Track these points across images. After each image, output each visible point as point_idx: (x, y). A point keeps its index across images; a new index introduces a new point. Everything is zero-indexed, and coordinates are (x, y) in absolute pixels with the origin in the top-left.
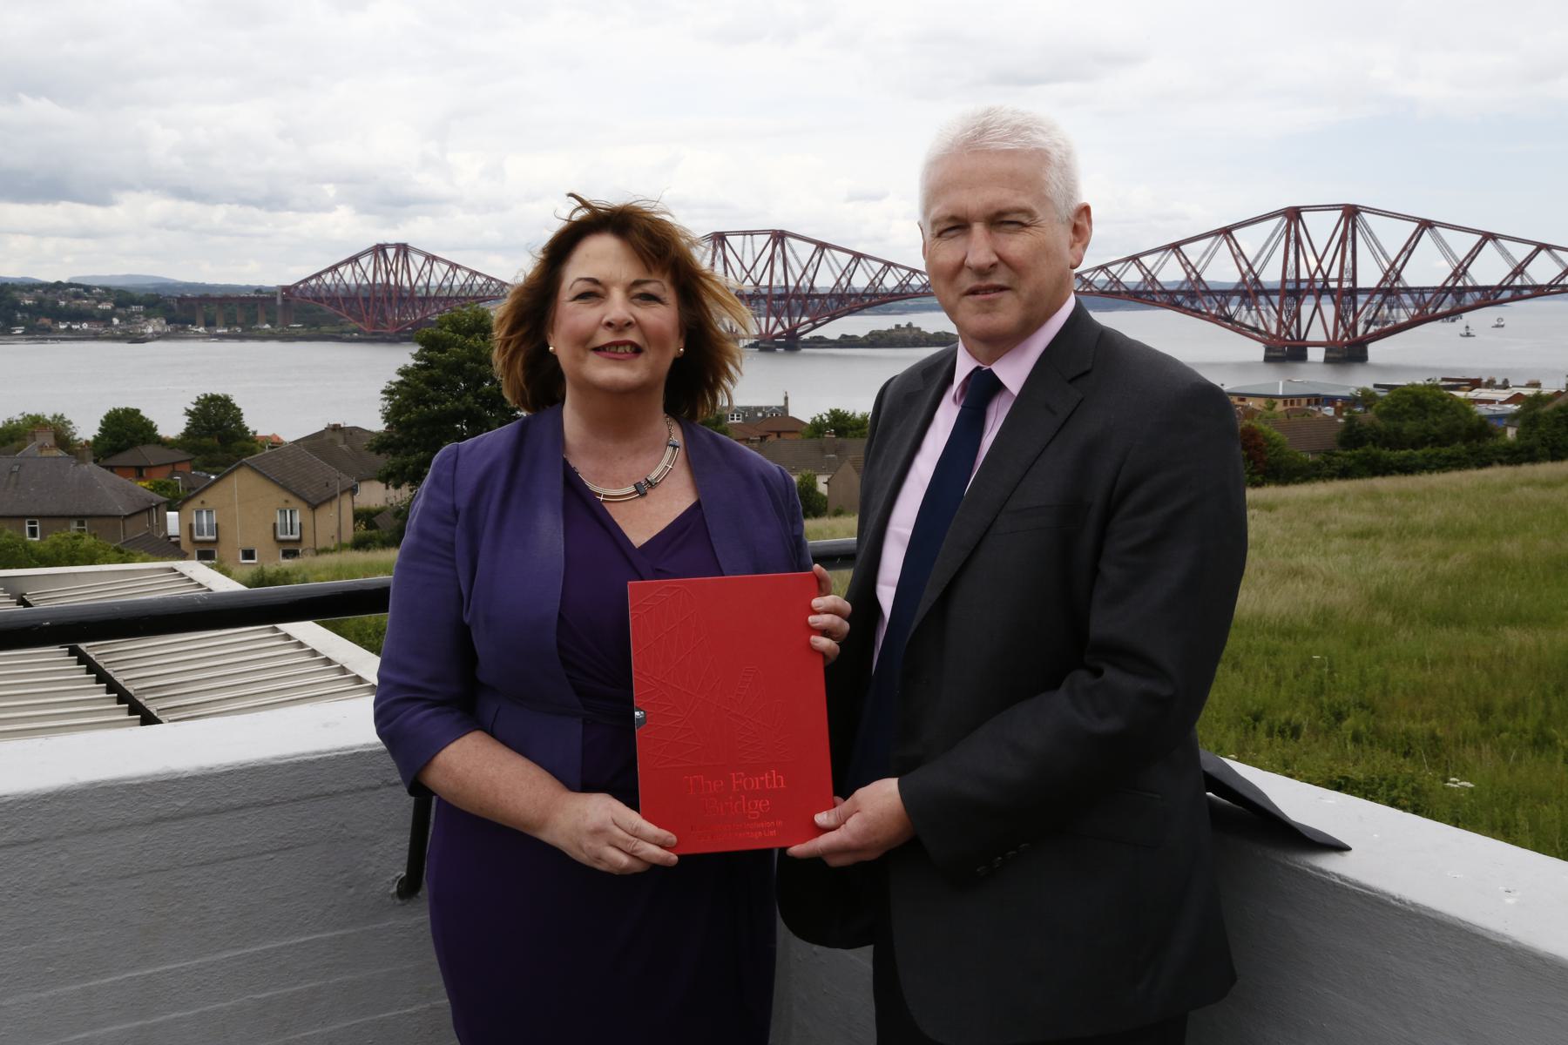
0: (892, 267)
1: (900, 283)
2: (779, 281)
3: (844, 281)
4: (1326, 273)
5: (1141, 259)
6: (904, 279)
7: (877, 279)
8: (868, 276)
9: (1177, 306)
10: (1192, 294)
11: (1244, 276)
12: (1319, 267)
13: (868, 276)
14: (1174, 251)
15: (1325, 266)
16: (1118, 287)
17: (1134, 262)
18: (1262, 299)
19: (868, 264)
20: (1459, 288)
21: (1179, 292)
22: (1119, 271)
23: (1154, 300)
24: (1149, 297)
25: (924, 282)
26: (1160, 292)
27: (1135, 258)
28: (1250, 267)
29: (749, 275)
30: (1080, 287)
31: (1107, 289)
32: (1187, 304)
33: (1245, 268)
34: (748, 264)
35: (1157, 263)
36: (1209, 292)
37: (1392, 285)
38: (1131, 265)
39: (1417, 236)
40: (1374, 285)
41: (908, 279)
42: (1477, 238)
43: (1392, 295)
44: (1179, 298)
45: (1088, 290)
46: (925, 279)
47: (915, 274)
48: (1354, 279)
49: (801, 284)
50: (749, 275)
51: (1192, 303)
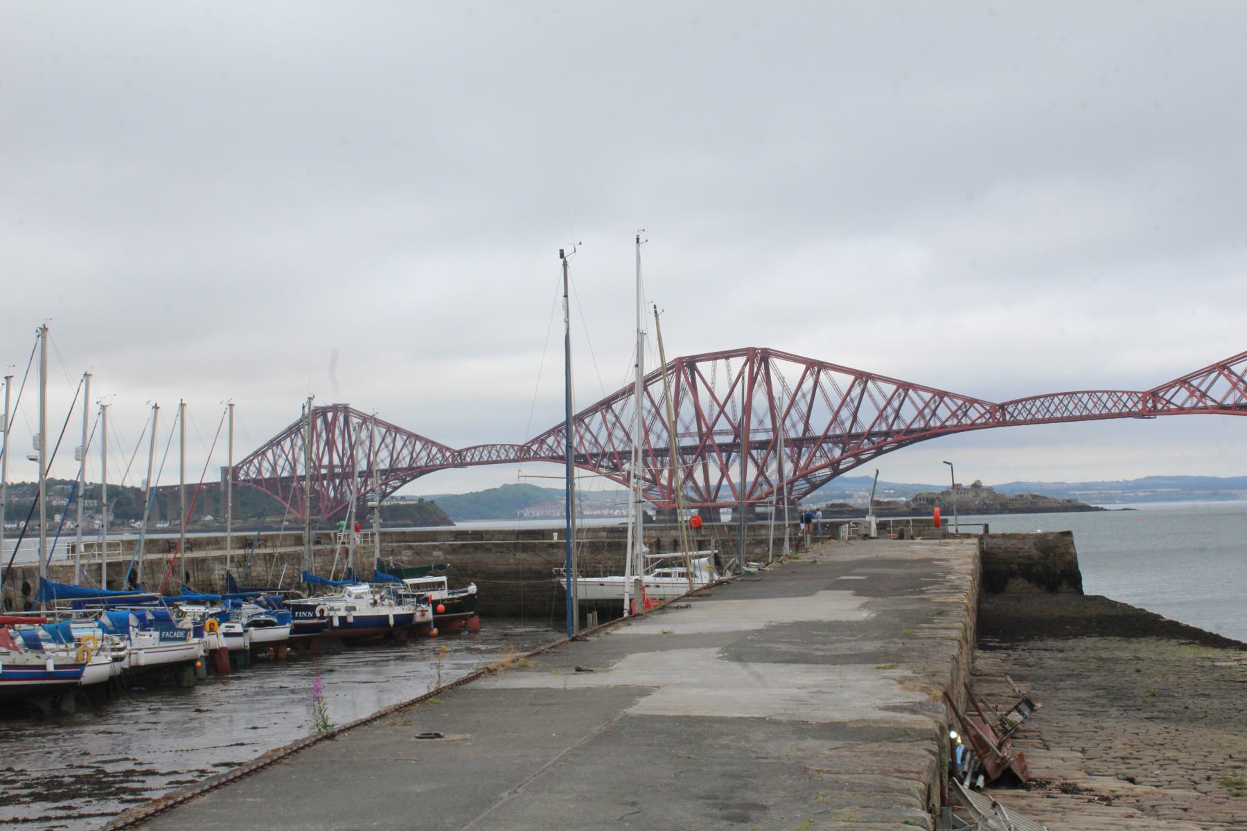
0: (911, 392)
1: (921, 413)
2: (761, 422)
3: (845, 414)
6: (927, 405)
7: (889, 410)
8: (915, 406)
13: (915, 406)
19: (878, 388)
25: (954, 408)
29: (722, 411)
30: (1187, 400)
34: (721, 395)
41: (933, 407)
45: (1201, 405)
46: (955, 404)
49: (788, 423)
50: (722, 411)
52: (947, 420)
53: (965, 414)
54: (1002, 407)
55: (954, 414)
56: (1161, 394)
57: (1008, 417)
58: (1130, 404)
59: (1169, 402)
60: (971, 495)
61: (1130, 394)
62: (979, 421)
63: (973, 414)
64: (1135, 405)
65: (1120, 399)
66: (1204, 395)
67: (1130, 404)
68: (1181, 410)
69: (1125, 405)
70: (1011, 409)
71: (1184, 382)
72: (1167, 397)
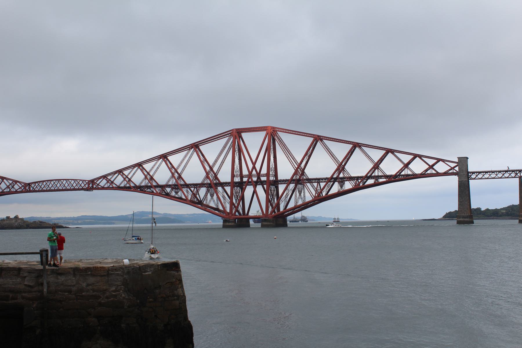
4: (258, 171)
5: (144, 166)
9: (168, 195)
10: (176, 187)
11: (207, 174)
12: (254, 167)
14: (164, 160)
15: (258, 166)
16: (129, 184)
17: (139, 168)
18: (220, 189)
20: (341, 178)
21: (169, 186)
22: (129, 174)
23: (153, 192)
24: (149, 190)
25: (8, 184)
26: (156, 187)
27: (139, 165)
28: (211, 168)
31: (122, 185)
32: (173, 194)
33: (208, 168)
35: (153, 167)
36: (187, 186)
37: (300, 177)
38: (136, 170)
39: (313, 146)
40: (289, 178)
42: (350, 146)
43: (301, 184)
44: (168, 190)
45: (111, 186)
46: (9, 182)
47: (3, 181)
48: (276, 175)
51: (177, 193)
52: (5, 189)
53: (13, 187)
54: (29, 184)
55: (8, 187)
56: (95, 182)
57: (31, 189)
58: (83, 185)
59: (98, 185)
60: (14, 221)
61: (83, 181)
62: (19, 190)
63: (16, 187)
64: (85, 185)
65: (79, 183)
66: (112, 182)
67: (83, 185)
68: (103, 188)
69: (81, 185)
70: (33, 185)
71: (104, 177)
72: (98, 183)
